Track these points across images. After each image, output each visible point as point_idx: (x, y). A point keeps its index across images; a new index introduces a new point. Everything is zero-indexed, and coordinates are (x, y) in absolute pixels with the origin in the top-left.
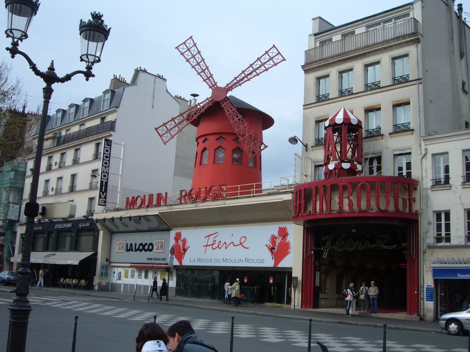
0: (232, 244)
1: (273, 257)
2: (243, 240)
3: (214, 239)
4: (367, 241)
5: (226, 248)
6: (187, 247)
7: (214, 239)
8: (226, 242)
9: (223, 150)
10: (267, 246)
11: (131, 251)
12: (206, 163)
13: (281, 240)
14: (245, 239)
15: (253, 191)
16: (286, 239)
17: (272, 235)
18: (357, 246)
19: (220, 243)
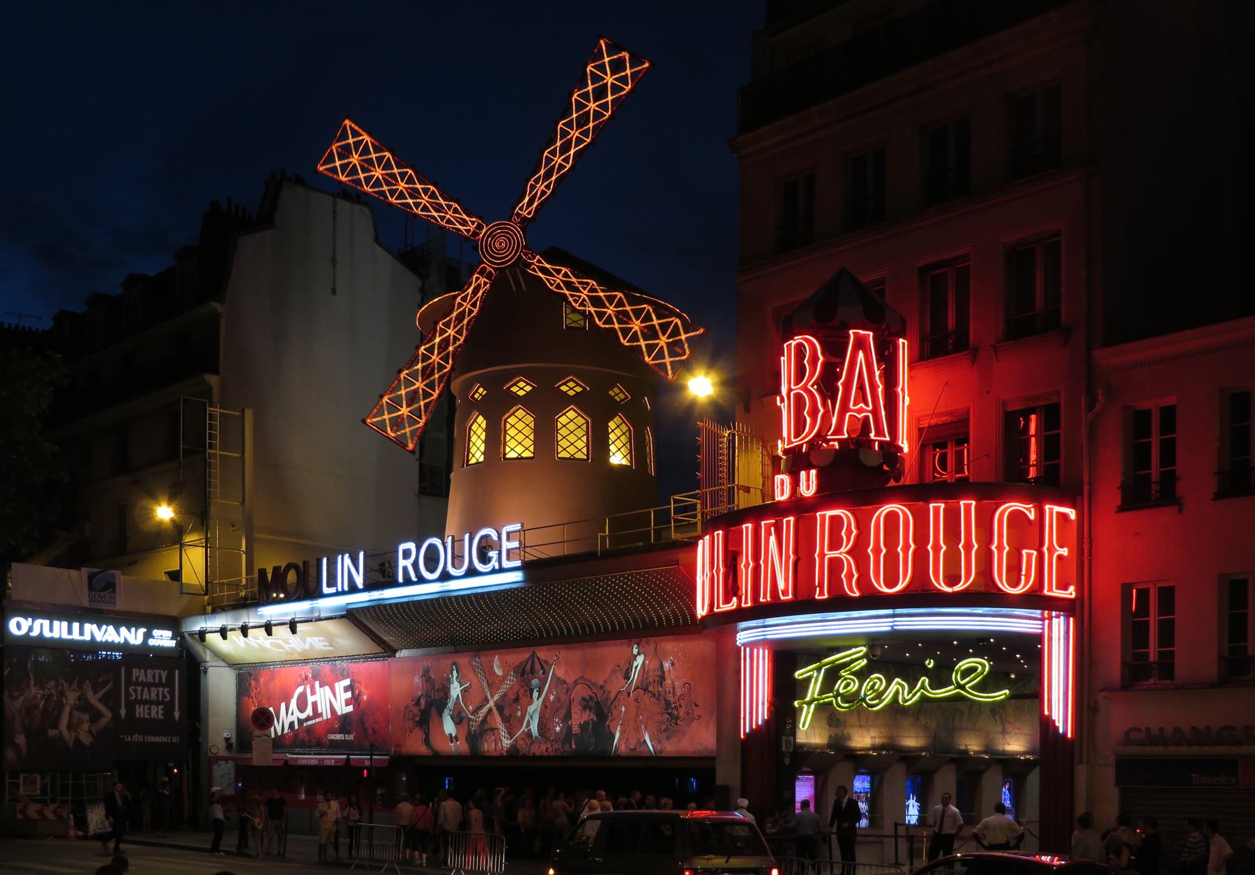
4: (923, 678)
9: (529, 419)
12: (481, 459)
15: (603, 538)
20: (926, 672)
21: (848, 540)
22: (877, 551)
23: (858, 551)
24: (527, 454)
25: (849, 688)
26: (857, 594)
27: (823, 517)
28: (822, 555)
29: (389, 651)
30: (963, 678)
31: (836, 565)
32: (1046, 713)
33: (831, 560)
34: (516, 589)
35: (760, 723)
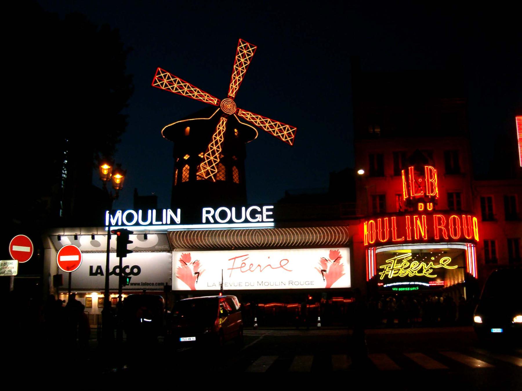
0: (269, 266)
1: (324, 278)
2: (283, 263)
3: (244, 262)
5: (261, 271)
6: (200, 270)
7: (244, 262)
8: (260, 265)
10: (316, 268)
11: (99, 275)
13: (333, 262)
14: (287, 261)
16: (339, 262)
17: (322, 257)
18: (422, 267)
19: (251, 266)
20: (432, 261)
21: (444, 224)
22: (451, 227)
23: (447, 226)
24: (222, 179)
25: (406, 265)
26: (447, 238)
27: (436, 217)
28: (436, 227)
29: (170, 249)
30: (443, 263)
31: (441, 230)
32: (468, 271)
33: (439, 228)
34: (270, 229)
35: (373, 276)
